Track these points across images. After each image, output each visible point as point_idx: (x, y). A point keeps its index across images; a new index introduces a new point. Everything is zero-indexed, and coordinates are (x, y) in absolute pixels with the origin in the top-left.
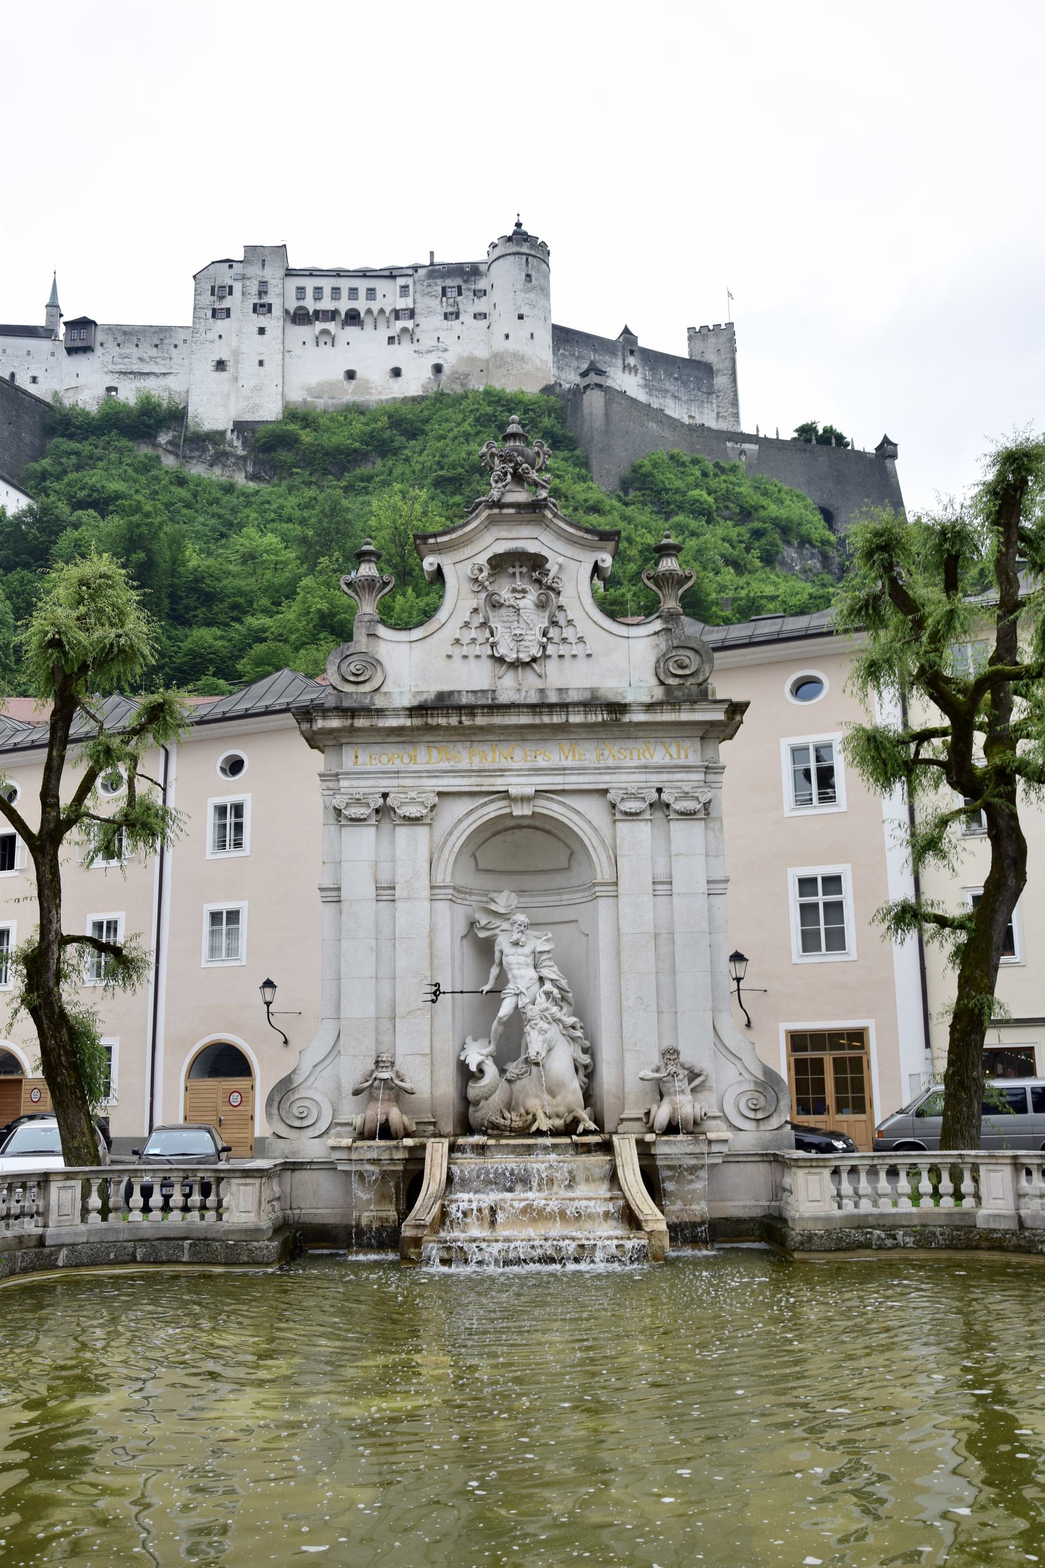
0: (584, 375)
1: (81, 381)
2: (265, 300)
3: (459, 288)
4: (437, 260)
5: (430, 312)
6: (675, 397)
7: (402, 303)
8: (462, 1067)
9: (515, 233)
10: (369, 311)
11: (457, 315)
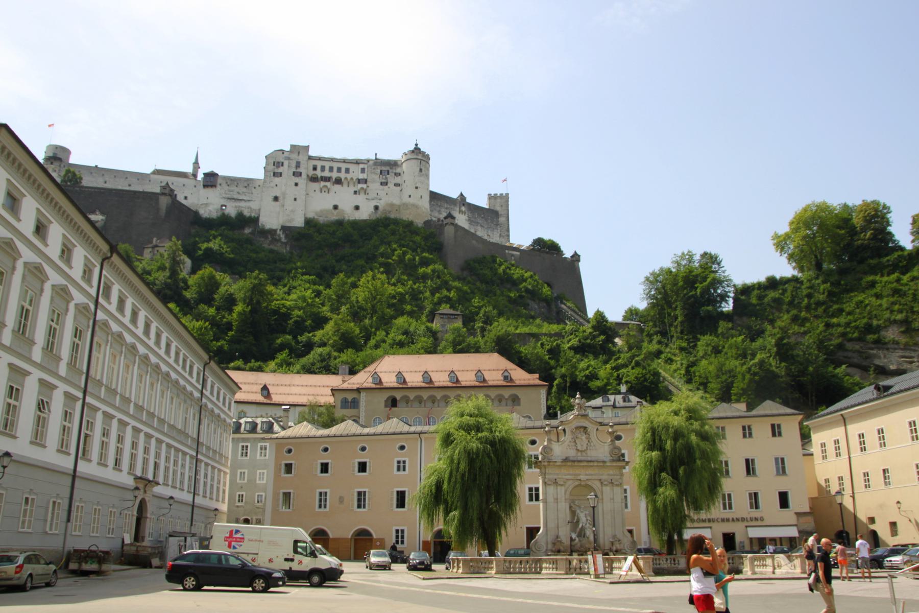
0: (446, 218)
1: (209, 201)
2: (299, 170)
3: (388, 171)
4: (378, 157)
5: (374, 181)
6: (482, 226)
7: (361, 176)
8: (571, 538)
9: (415, 148)
10: (346, 178)
11: (386, 184)
